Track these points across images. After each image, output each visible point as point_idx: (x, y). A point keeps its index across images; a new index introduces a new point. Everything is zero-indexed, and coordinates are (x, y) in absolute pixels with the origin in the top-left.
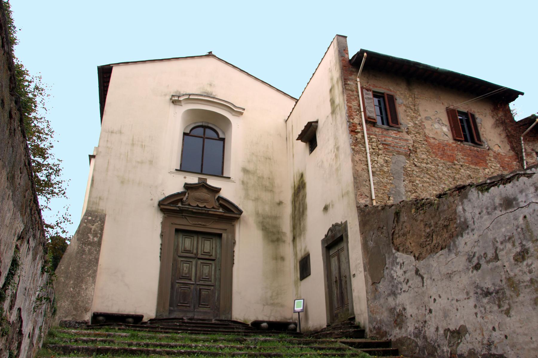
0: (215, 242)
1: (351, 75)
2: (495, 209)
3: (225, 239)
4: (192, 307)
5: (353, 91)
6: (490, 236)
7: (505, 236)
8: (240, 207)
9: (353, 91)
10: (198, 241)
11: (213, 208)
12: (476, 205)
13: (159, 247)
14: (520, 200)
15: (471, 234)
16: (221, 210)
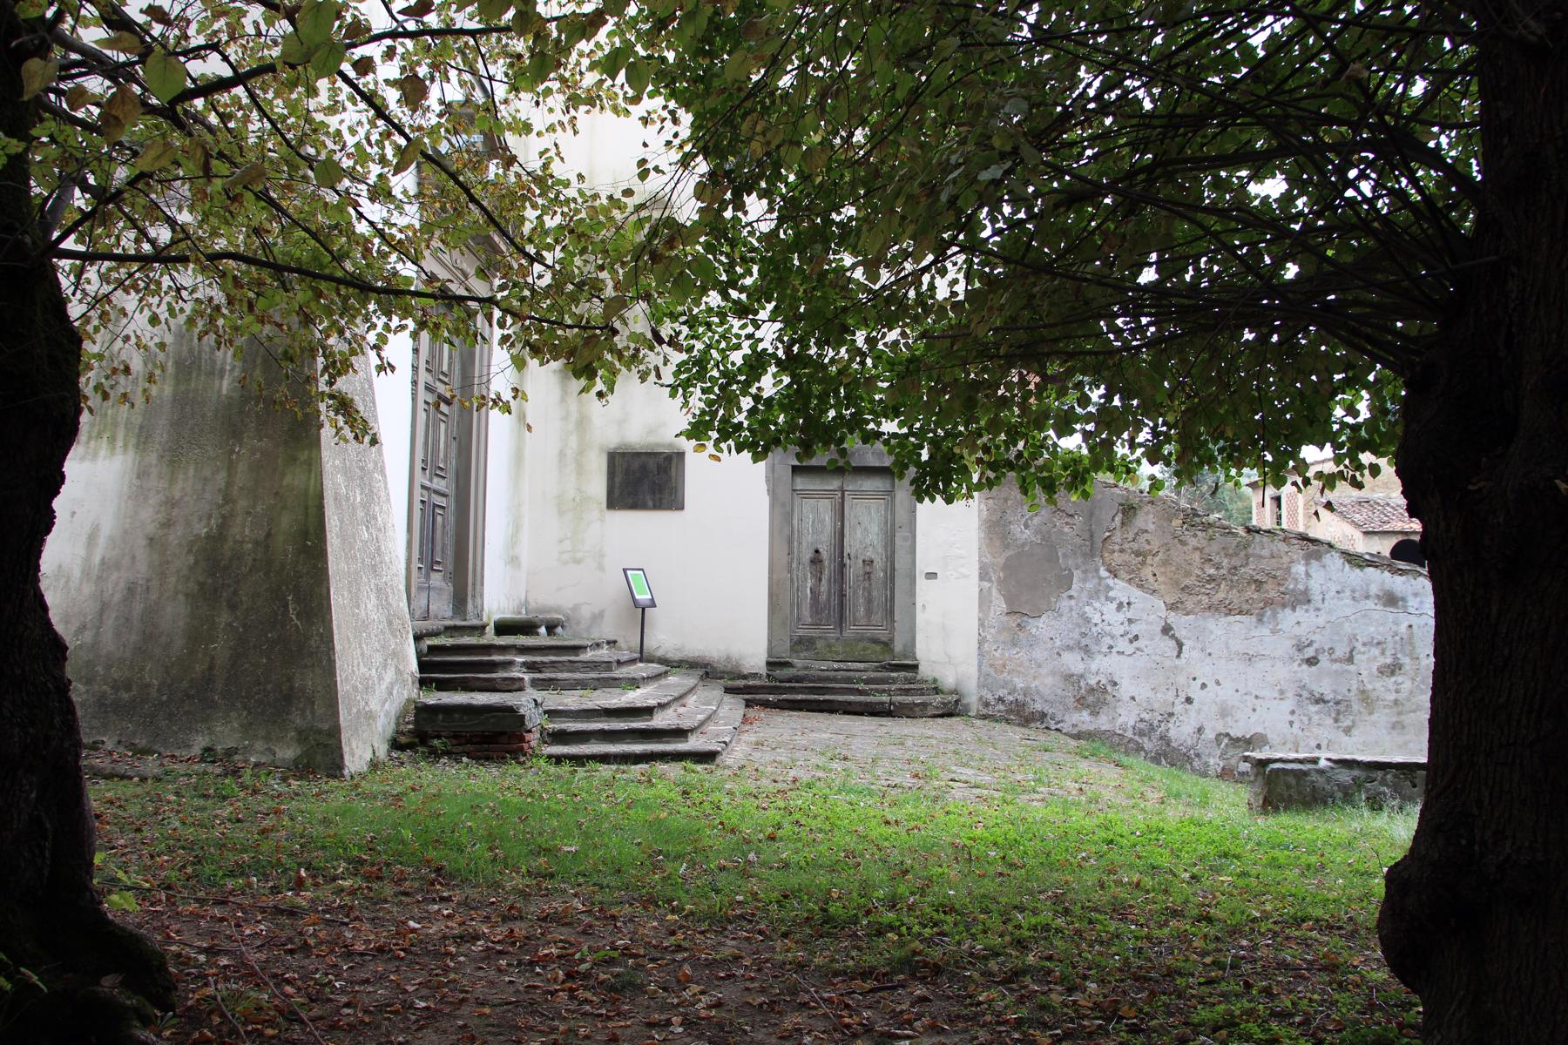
2: (1367, 597)
6: (1348, 628)
7: (1373, 638)
12: (1334, 578)
14: (1410, 604)
15: (1313, 614)
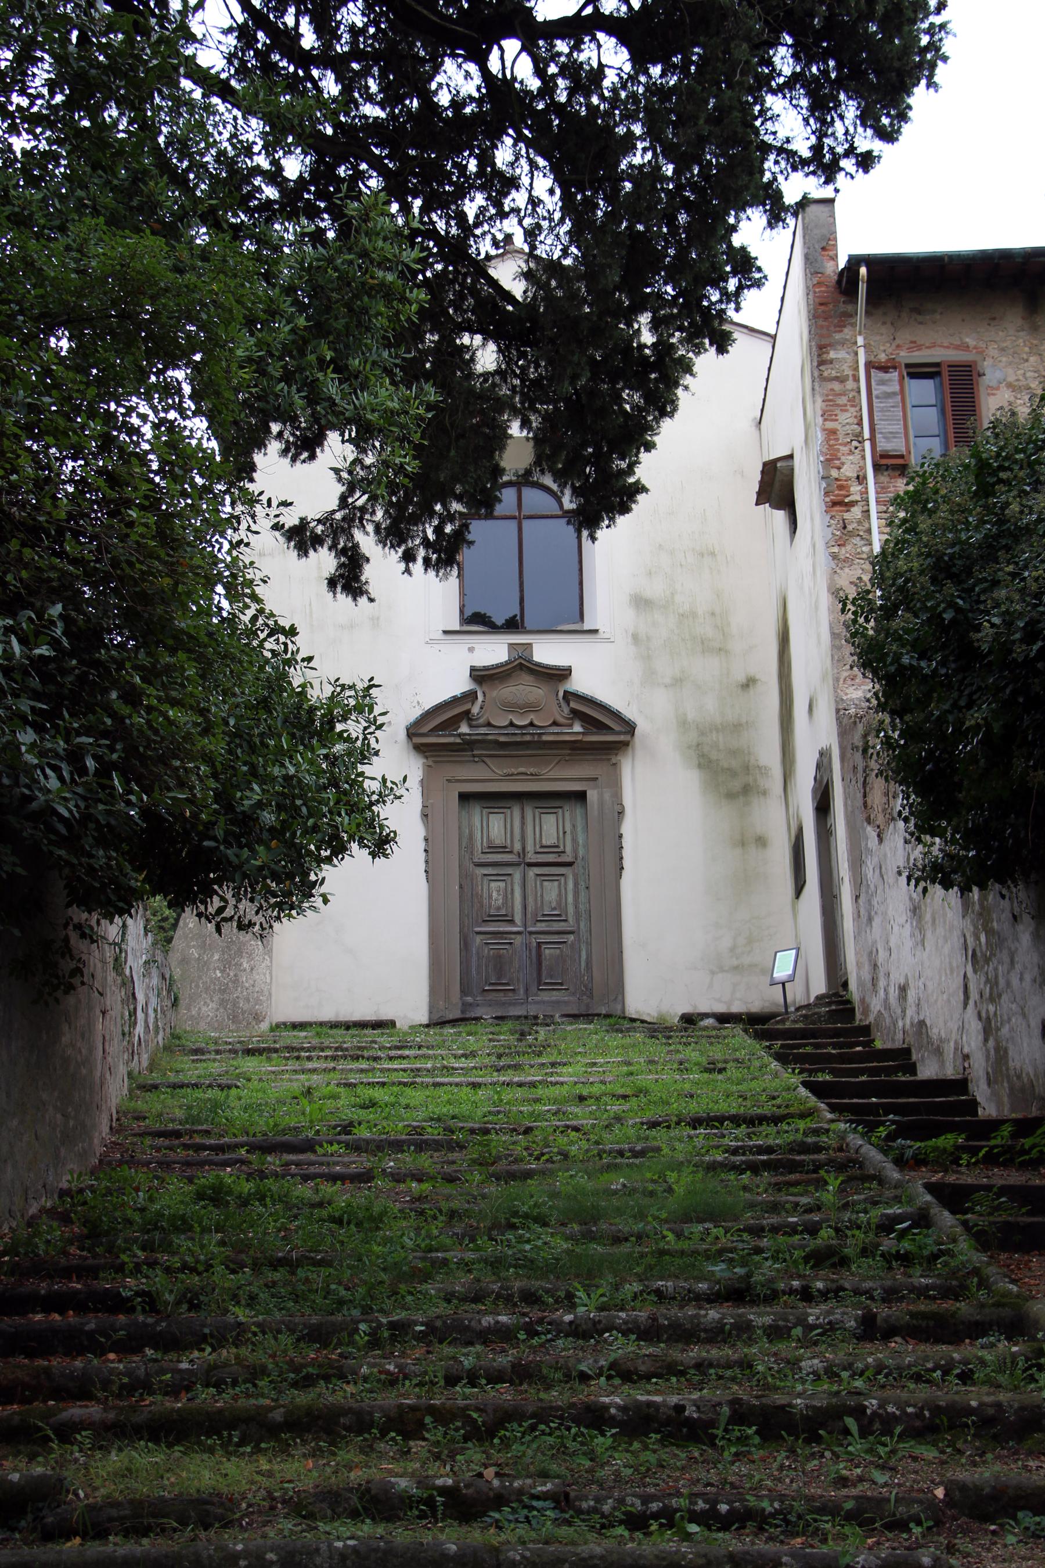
0: (570, 813)
1: (841, 326)
4: (522, 991)
5: (841, 380)
8: (629, 712)
9: (841, 380)
10: (523, 817)
11: (555, 723)
13: (422, 845)
16: (577, 728)
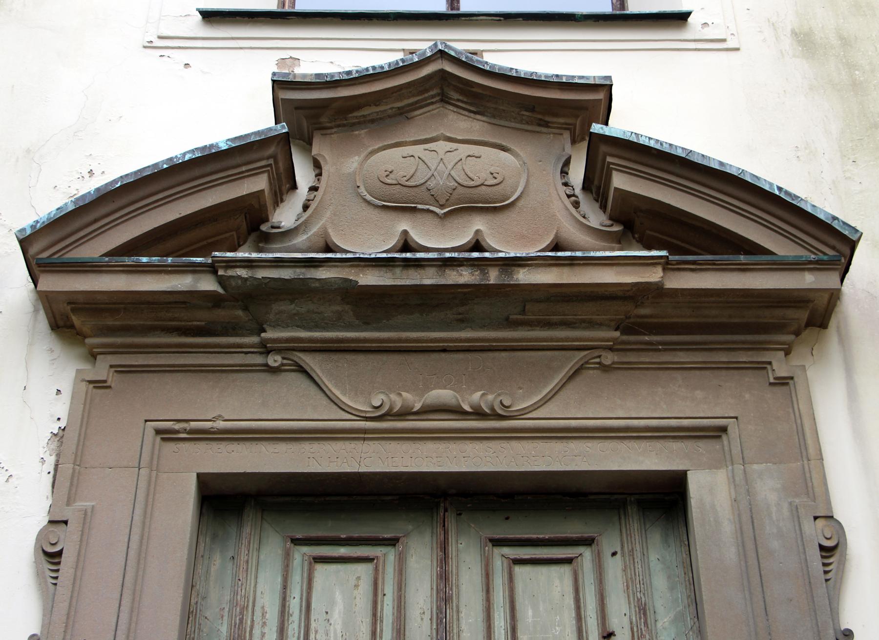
3: (728, 528)
